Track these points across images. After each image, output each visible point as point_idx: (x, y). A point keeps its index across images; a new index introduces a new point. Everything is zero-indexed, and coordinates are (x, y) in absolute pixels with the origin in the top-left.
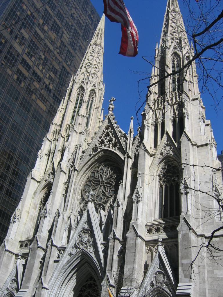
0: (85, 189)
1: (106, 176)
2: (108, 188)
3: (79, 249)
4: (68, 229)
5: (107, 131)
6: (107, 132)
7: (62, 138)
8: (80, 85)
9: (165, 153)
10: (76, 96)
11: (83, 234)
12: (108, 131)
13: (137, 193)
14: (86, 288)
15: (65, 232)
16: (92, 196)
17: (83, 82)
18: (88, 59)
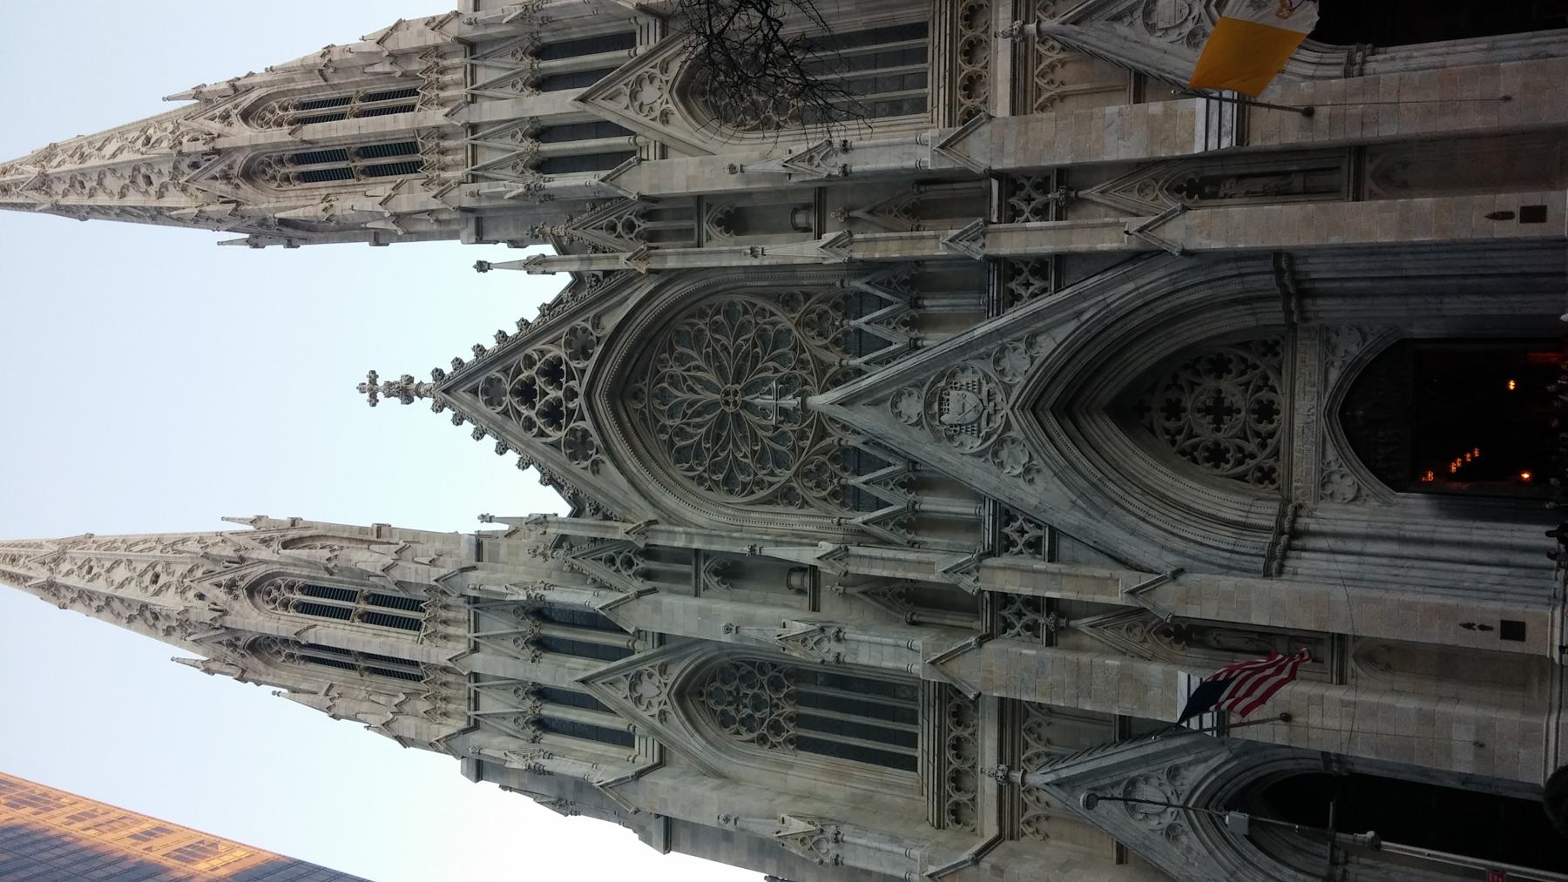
0: (745, 485)
1: (708, 386)
2: (759, 366)
3: (1008, 426)
4: (910, 537)
5: (507, 399)
6: (514, 392)
7: (475, 655)
8: (242, 594)
9: (667, 103)
10: (292, 612)
11: (942, 419)
12: (508, 389)
13: (811, 159)
14: (1180, 431)
16: (782, 394)
17: (231, 587)
18: (122, 585)
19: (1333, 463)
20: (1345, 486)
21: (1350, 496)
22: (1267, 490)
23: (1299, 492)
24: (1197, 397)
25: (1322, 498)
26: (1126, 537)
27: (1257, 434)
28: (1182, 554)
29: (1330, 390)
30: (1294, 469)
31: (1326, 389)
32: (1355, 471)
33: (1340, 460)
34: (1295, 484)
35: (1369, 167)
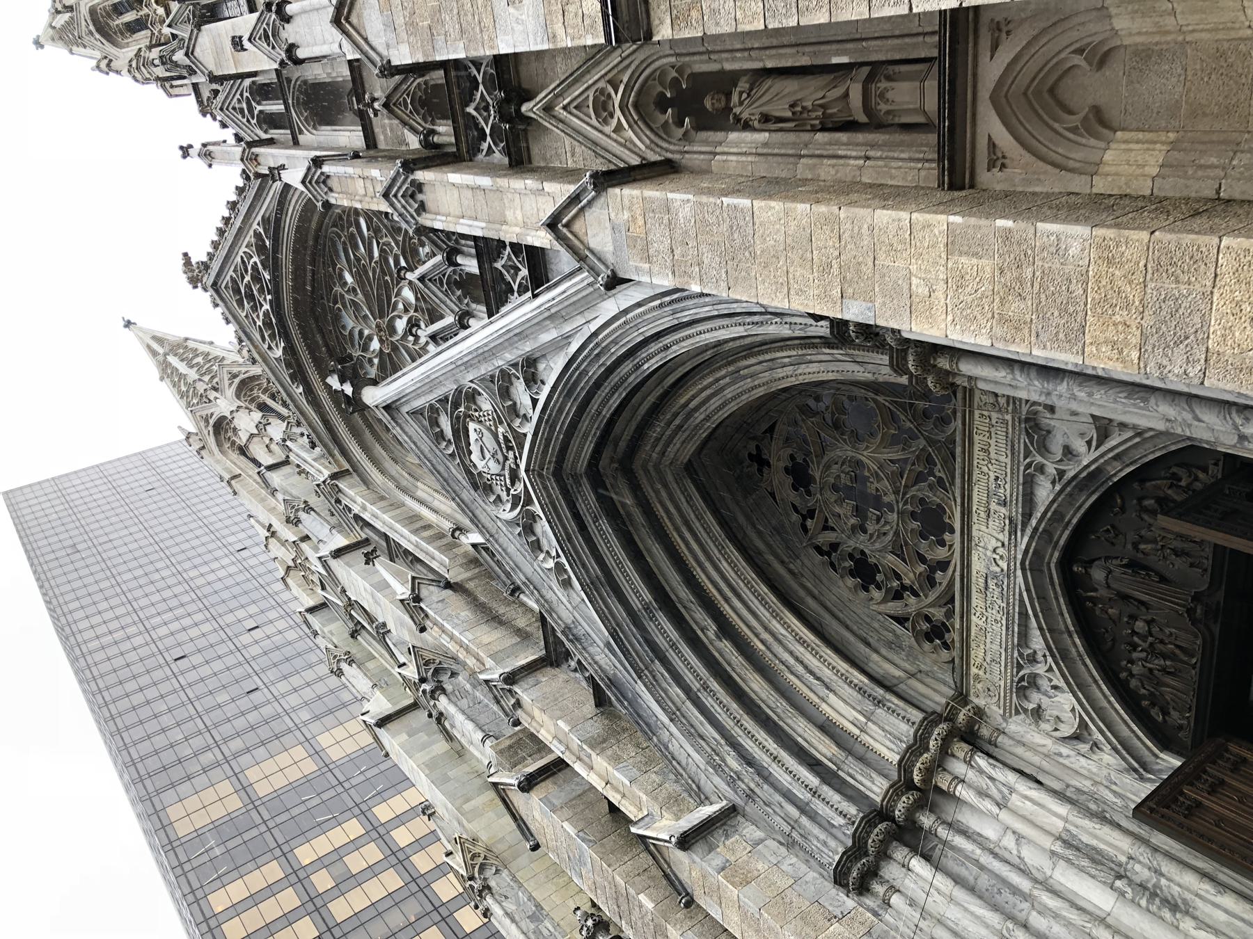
8: (210, 428)
14: (811, 514)
15: (522, 596)
19: (1040, 657)
20: (1063, 704)
21: (1067, 730)
22: (932, 659)
23: (979, 686)
24: (828, 467)
25: (1017, 713)
26: (665, 720)
27: (923, 559)
28: (733, 781)
29: (1034, 522)
30: (973, 645)
31: (1027, 516)
32: (1079, 686)
33: (1050, 659)
34: (974, 670)
35: (991, 70)
